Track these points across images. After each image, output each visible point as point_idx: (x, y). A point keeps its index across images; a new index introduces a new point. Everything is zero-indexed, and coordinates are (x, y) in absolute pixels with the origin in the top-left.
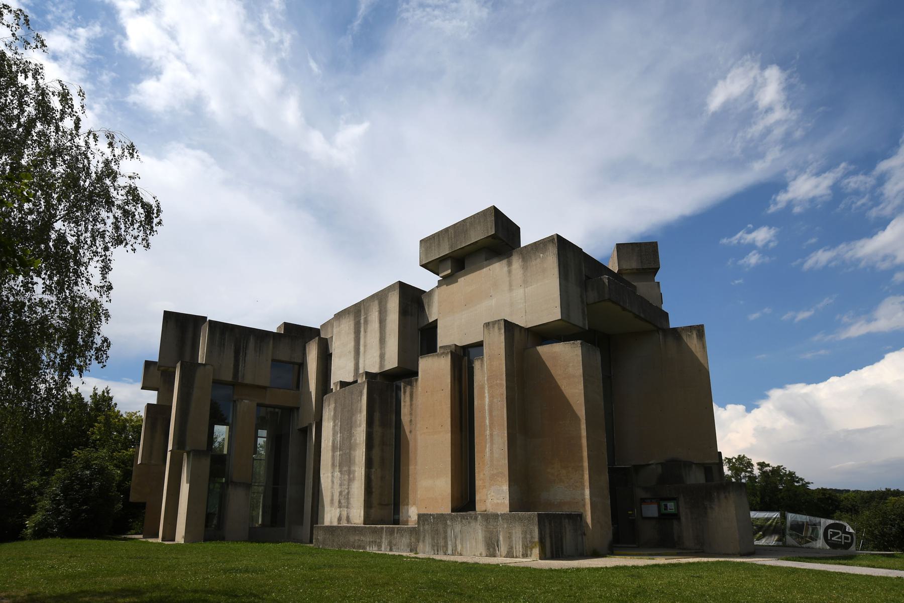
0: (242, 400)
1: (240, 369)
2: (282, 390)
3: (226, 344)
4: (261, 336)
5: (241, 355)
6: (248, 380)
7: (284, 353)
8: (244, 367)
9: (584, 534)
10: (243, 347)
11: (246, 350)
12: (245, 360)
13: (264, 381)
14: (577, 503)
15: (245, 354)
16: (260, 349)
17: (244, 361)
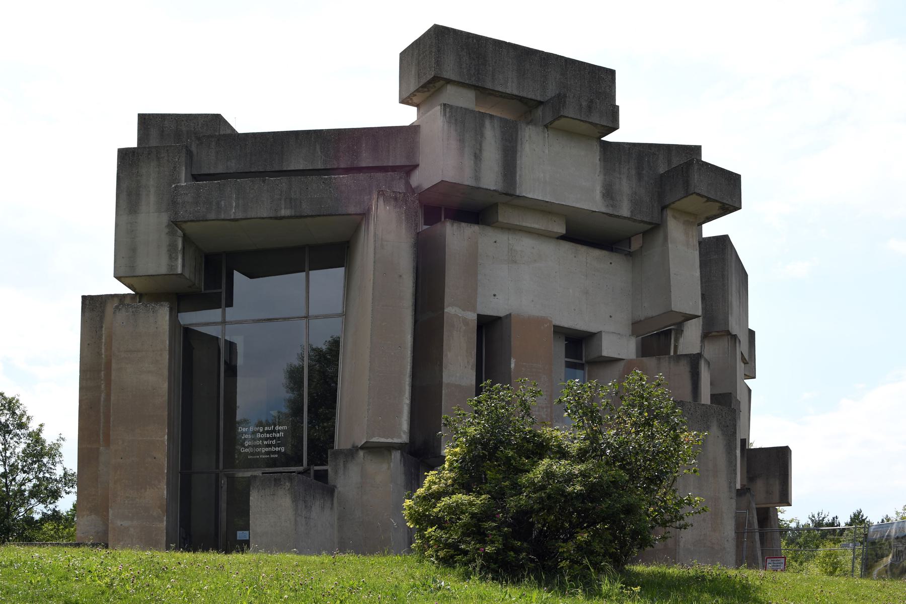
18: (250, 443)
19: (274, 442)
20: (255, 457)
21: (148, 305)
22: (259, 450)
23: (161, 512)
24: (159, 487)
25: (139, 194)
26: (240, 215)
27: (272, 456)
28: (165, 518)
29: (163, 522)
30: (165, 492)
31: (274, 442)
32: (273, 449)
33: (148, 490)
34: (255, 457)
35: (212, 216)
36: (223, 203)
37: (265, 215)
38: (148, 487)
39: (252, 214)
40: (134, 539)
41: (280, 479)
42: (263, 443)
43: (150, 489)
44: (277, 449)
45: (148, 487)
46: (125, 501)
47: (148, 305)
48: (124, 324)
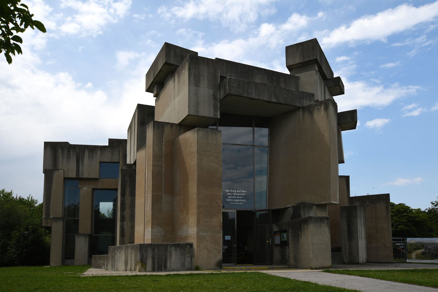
0: (83, 188)
1: (80, 170)
2: (107, 179)
3: (71, 156)
4: (93, 149)
5: (81, 161)
6: (85, 176)
7: (107, 157)
8: (83, 168)
9: (193, 256)
10: (82, 157)
11: (83, 159)
12: (83, 164)
13: (95, 175)
14: (191, 236)
15: (83, 160)
16: (92, 158)
17: (82, 165)
18: (230, 197)
19: (241, 197)
20: (233, 203)
21: (213, 131)
22: (234, 200)
23: (220, 229)
24: (219, 216)
25: (200, 78)
26: (256, 97)
27: (241, 203)
28: (222, 232)
29: (221, 233)
30: (222, 219)
31: (241, 197)
32: (241, 200)
33: (214, 218)
34: (233, 203)
35: (245, 95)
36: (249, 90)
37: (266, 99)
38: (214, 216)
39: (261, 98)
40: (208, 242)
41: (323, 219)
42: (236, 197)
43: (215, 217)
44: (242, 200)
45: (214, 216)
46: (204, 223)
47: (213, 131)
48: (202, 137)
